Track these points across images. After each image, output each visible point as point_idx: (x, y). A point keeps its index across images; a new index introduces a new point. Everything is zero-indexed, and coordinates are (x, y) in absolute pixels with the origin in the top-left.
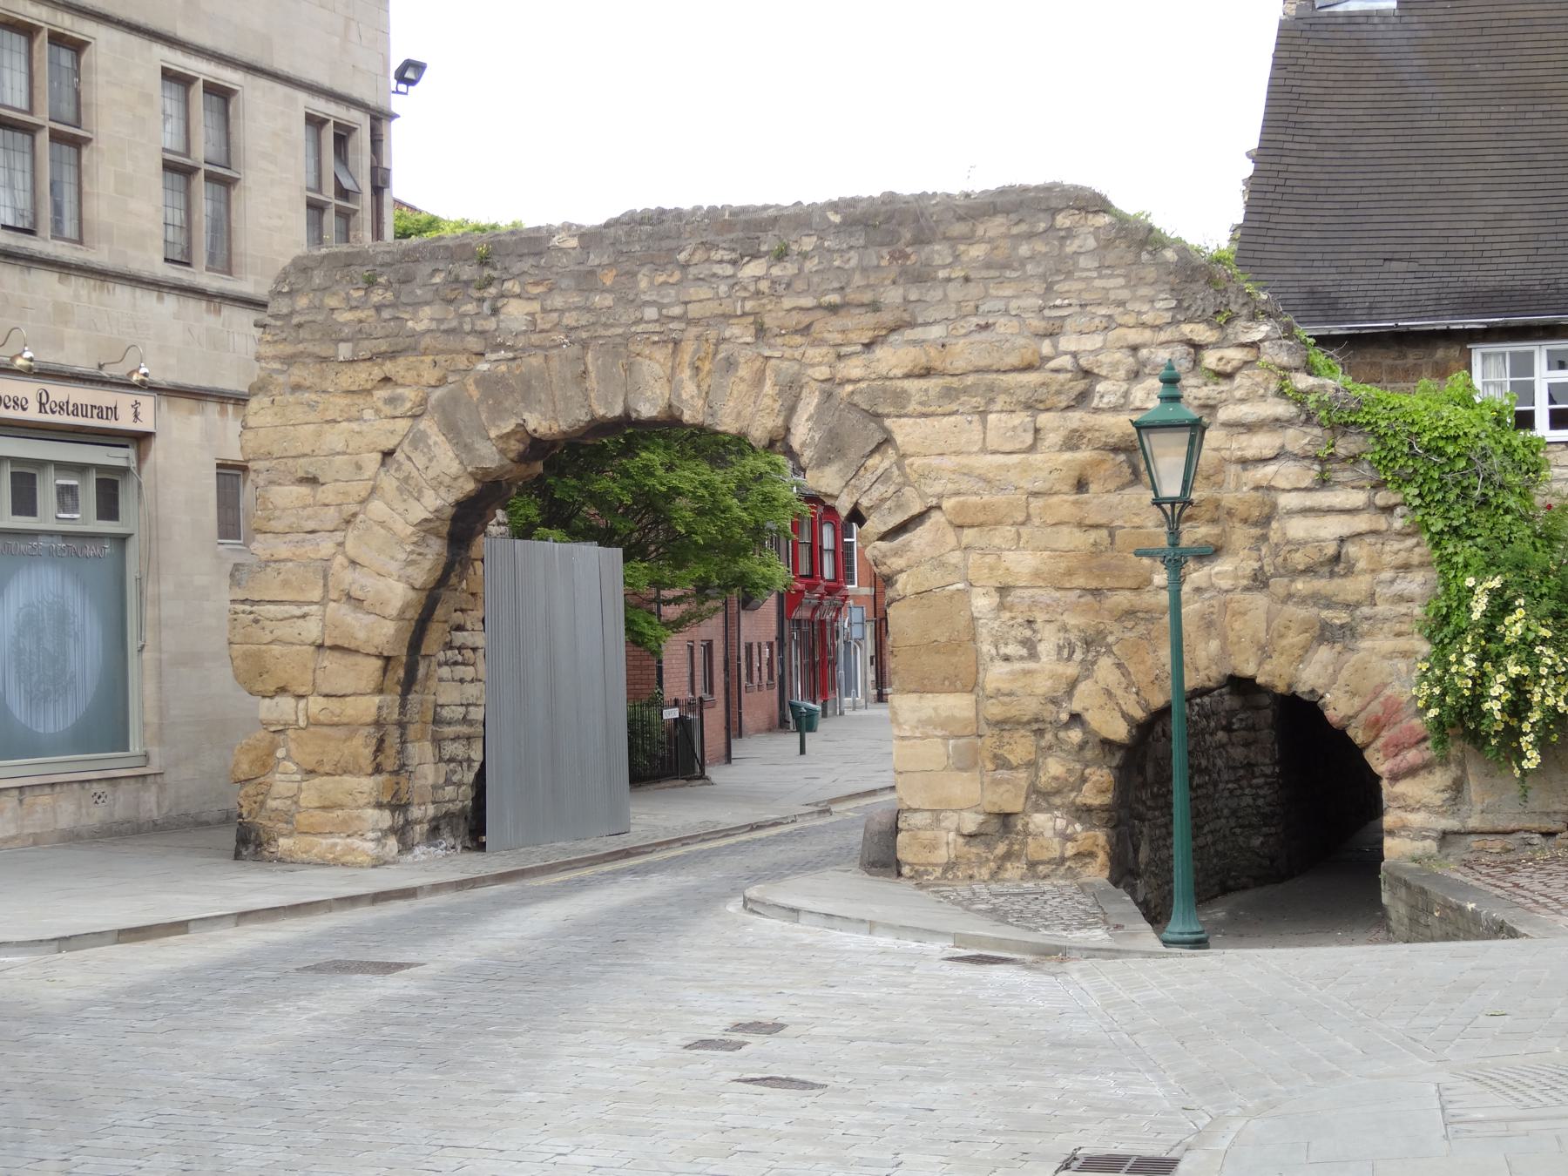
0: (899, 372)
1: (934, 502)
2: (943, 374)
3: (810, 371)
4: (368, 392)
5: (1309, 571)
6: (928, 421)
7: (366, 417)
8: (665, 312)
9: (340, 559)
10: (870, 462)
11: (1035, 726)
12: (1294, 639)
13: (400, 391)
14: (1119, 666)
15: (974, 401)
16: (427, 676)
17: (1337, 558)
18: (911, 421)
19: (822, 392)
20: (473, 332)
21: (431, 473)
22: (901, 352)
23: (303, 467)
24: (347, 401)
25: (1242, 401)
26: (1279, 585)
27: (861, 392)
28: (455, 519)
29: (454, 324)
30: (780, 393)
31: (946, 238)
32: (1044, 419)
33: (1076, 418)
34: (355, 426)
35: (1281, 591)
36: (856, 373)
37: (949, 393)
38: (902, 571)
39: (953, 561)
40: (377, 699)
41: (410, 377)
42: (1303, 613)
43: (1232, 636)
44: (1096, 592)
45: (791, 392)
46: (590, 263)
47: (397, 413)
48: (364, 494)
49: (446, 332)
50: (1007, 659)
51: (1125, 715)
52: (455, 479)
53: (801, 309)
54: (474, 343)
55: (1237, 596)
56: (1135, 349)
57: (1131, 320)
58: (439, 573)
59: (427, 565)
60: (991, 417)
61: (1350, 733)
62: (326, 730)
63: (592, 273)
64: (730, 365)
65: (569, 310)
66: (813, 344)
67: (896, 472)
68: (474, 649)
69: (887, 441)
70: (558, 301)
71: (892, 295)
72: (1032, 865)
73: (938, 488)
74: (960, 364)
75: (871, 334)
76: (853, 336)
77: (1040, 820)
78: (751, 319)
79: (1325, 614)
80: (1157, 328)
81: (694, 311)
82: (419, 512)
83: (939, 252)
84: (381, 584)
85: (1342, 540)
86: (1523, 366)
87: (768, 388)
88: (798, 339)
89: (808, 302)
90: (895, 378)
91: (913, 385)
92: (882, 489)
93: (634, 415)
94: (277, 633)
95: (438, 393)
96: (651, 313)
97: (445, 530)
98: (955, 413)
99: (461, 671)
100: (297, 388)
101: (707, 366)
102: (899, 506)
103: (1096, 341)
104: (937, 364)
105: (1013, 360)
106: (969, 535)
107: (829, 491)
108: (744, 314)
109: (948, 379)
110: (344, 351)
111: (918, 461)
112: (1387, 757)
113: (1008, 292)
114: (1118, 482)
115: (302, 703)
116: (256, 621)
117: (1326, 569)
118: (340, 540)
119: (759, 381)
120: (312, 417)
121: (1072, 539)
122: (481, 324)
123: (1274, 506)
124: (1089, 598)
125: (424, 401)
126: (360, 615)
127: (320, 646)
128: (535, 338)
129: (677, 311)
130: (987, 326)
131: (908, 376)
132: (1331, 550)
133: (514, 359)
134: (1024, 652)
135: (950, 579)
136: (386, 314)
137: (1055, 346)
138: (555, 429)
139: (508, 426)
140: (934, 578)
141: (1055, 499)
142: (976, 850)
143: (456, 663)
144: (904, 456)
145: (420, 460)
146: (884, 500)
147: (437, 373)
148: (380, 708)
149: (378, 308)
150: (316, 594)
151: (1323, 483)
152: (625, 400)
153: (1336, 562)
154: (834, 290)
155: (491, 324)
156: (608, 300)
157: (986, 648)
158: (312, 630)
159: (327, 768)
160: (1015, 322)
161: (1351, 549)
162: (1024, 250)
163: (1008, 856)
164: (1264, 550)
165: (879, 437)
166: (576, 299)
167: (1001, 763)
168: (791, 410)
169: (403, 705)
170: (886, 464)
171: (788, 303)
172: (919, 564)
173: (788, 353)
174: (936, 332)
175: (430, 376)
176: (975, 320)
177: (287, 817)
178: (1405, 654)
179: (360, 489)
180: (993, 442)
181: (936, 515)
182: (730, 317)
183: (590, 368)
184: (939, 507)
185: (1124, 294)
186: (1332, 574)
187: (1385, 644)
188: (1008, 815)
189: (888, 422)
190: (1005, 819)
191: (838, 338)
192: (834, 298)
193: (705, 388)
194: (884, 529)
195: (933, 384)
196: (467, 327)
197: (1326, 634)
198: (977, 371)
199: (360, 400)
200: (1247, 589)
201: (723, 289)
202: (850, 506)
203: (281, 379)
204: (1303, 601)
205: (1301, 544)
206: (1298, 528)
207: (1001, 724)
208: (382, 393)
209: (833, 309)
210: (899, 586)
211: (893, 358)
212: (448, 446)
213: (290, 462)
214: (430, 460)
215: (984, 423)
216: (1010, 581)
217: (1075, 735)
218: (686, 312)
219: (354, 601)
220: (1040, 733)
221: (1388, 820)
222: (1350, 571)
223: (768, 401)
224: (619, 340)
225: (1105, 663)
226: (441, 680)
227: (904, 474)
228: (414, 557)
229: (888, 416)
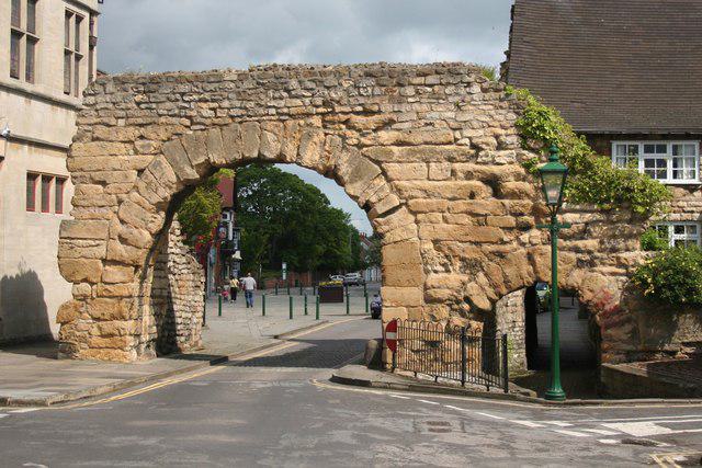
0: (389, 143)
1: (404, 201)
11: (448, 302)
14: (486, 275)
20: (186, 117)
23: (98, 176)
24: (122, 145)
29: (177, 111)
31: (410, 84)
32: (457, 166)
33: (471, 166)
34: (126, 158)
36: (369, 142)
37: (414, 153)
41: (153, 136)
42: (573, 256)
44: (477, 243)
50: (436, 272)
54: (188, 122)
55: (543, 247)
57: (496, 124)
60: (433, 165)
62: (108, 300)
69: (384, 173)
70: (226, 104)
71: (387, 107)
74: (419, 139)
79: (580, 255)
81: (293, 111)
82: (156, 199)
83: (410, 91)
84: (135, 231)
85: (587, 224)
89: (347, 109)
94: (83, 253)
96: (273, 111)
100: (98, 139)
103: (481, 132)
105: (442, 139)
106: (420, 216)
110: (121, 122)
115: (94, 287)
116: (72, 248)
120: (105, 152)
121: (467, 220)
122: (189, 113)
124: (474, 246)
127: (105, 261)
128: (216, 121)
129: (286, 110)
130: (431, 124)
136: (143, 106)
137: (461, 134)
139: (202, 159)
141: (459, 201)
142: (415, 357)
149: (138, 104)
150: (105, 235)
154: (360, 105)
155: (194, 113)
158: (101, 251)
159: (106, 317)
162: (448, 90)
163: (436, 360)
166: (238, 104)
169: (141, 288)
174: (406, 126)
177: (83, 339)
184: (406, 204)
185: (493, 112)
186: (582, 238)
190: (433, 344)
192: (360, 109)
197: (580, 264)
198: (426, 143)
201: (307, 101)
203: (89, 134)
205: (567, 225)
206: (569, 217)
208: (139, 143)
211: (385, 136)
213: (93, 174)
215: (428, 167)
216: (438, 237)
217: (466, 306)
219: (123, 240)
220: (450, 305)
225: (481, 274)
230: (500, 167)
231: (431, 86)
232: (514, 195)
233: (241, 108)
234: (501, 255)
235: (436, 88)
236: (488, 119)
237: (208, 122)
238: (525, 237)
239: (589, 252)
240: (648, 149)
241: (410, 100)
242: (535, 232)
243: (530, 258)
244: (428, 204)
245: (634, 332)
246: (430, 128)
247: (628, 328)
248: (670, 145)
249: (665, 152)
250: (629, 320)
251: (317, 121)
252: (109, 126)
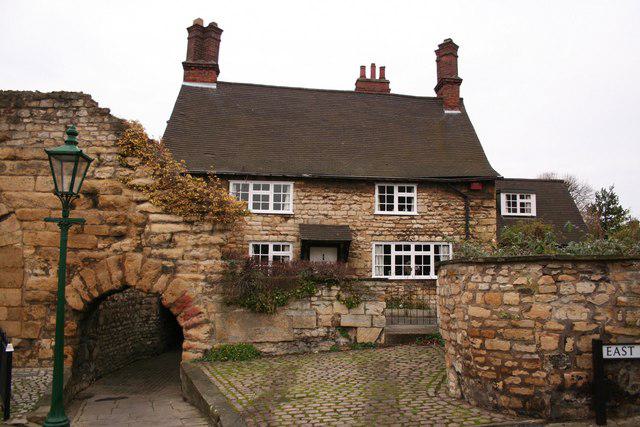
1: (12, 210)
2: (20, 159)
5: (159, 246)
12: (153, 272)
15: (33, 170)
17: (170, 241)
25: (138, 177)
26: (148, 250)
31: (28, 107)
35: (148, 253)
37: (23, 167)
43: (127, 270)
50: (36, 275)
51: (83, 300)
56: (98, 155)
57: (98, 143)
61: (171, 310)
72: (40, 360)
77: (44, 342)
79: (164, 262)
80: (107, 147)
83: (25, 113)
85: (172, 234)
86: (246, 188)
91: (8, 163)
104: (19, 156)
111: (8, 193)
112: (185, 320)
113: (51, 129)
114: (88, 206)
117: (166, 245)
123: (148, 219)
130: (41, 142)
131: (5, 159)
132: (168, 237)
134: (44, 273)
140: (10, 241)
151: (166, 212)
153: (171, 242)
157: (28, 270)
160: (52, 141)
161: (176, 237)
162: (59, 114)
164: (142, 236)
167: (30, 317)
178: (195, 280)
180: (39, 188)
181: (13, 216)
185: (96, 133)
186: (168, 247)
187: (187, 276)
188: (32, 340)
190: (31, 340)
195: (16, 163)
197: (165, 270)
198: (35, 159)
200: (134, 251)
204: (156, 257)
206: (156, 228)
207: (33, 301)
216: (40, 244)
221: (185, 344)
222: (175, 246)
230: (101, 182)
231: (45, 109)
232: (110, 207)
234: (95, 260)
235: (50, 111)
236: (92, 139)
238: (116, 245)
239: (173, 260)
240: (256, 188)
241: (25, 120)
242: (127, 241)
243: (121, 265)
244: (32, 213)
245: (212, 332)
246: (38, 145)
247: (206, 328)
248: (272, 185)
249: (268, 189)
250: (207, 322)
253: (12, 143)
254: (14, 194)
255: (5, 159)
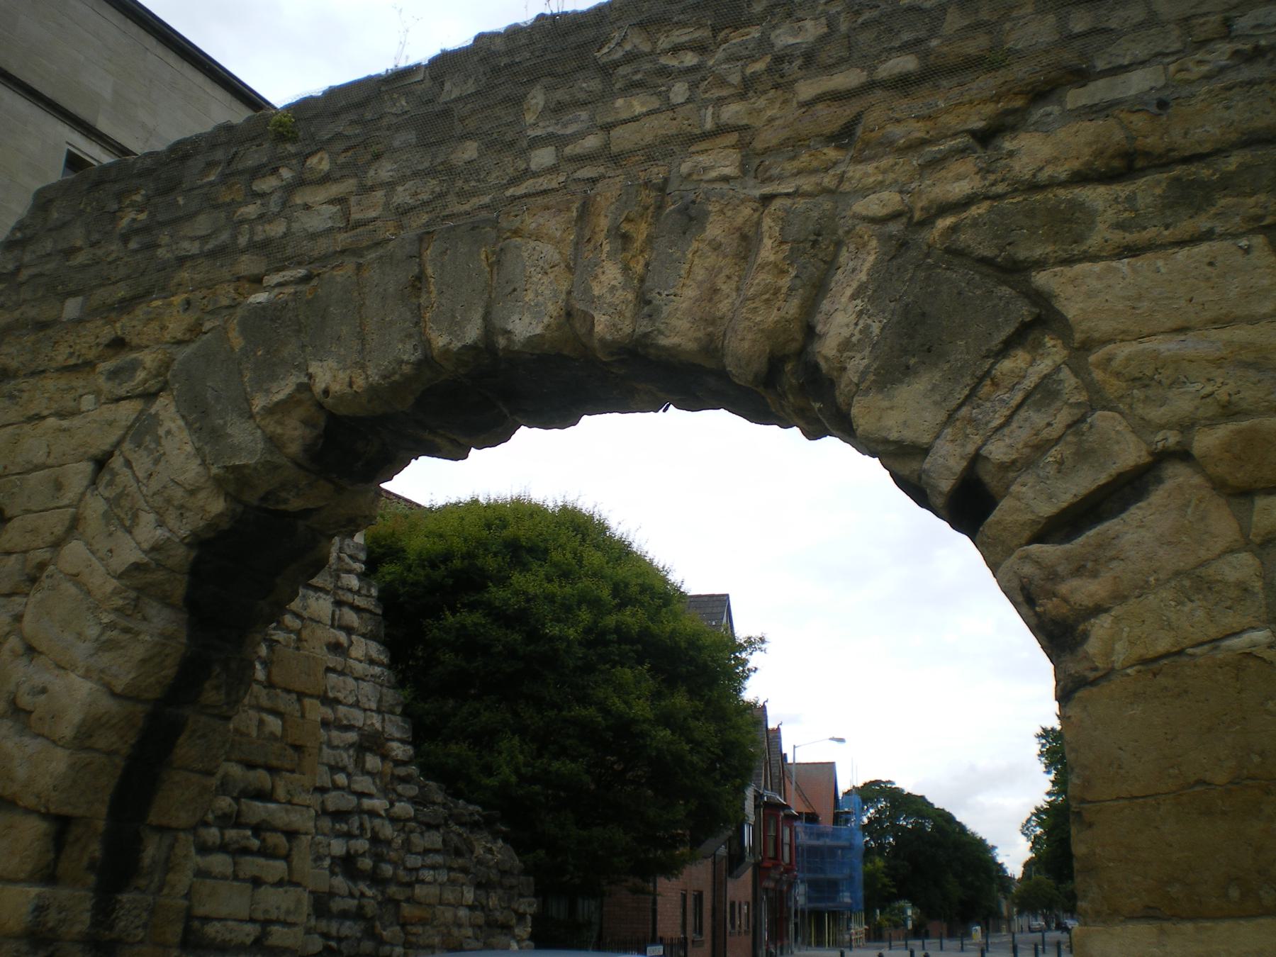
0: (1062, 172)
1: (1172, 439)
2: (1162, 161)
3: (860, 207)
4: (89, 365)
6: (1140, 262)
7: (84, 407)
8: (568, 150)
9: (13, 642)
10: (1006, 365)
13: (134, 355)
16: (168, 865)
18: (1098, 267)
19: (885, 239)
21: (154, 485)
22: (1062, 134)
27: (975, 223)
28: (196, 572)
29: (224, 236)
30: (791, 258)
36: (960, 189)
37: (1190, 196)
38: (1098, 610)
39: (1232, 576)
40: (34, 891)
45: (817, 252)
46: (444, 98)
47: (122, 391)
48: (59, 530)
49: (212, 254)
52: (192, 493)
53: (836, 97)
58: (170, 671)
59: (139, 652)
63: (446, 113)
64: (691, 218)
65: (403, 179)
66: (857, 160)
67: (1069, 380)
68: (292, 834)
69: (1043, 319)
70: (385, 171)
73: (1182, 404)
75: (989, 109)
76: (951, 121)
78: (733, 138)
81: (624, 138)
82: (129, 552)
87: (767, 252)
88: (831, 153)
90: (1052, 183)
91: (1095, 196)
92: (1039, 419)
93: (502, 342)
95: (188, 350)
96: (543, 157)
97: (179, 590)
98: (1208, 236)
99: (252, 865)
101: (641, 231)
102: (1084, 455)
104: (1152, 142)
107: (909, 435)
108: (721, 130)
109: (1178, 171)
110: (72, 308)
111: (1124, 351)
118: (19, 609)
119: (747, 241)
125: (166, 365)
126: (27, 740)
129: (592, 142)
131: (1081, 178)
133: (307, 279)
135: (1231, 620)
138: (360, 382)
139: (284, 389)
140: (1194, 620)
143: (246, 851)
144: (1087, 346)
145: (142, 463)
146: (1041, 447)
147: (189, 318)
148: (40, 909)
152: (487, 317)
154: (904, 48)
155: (276, 229)
156: (470, 150)
165: (1025, 311)
168: (819, 289)
169: (104, 910)
170: (1044, 366)
171: (806, 90)
172: (1143, 589)
173: (807, 184)
174: (1138, 82)
175: (176, 325)
176: (1226, 48)
179: (55, 522)
181: (1178, 476)
182: (692, 139)
183: (429, 271)
184: (1183, 455)
189: (1041, 279)
191: (918, 130)
193: (639, 268)
194: (1047, 509)
196: (243, 241)
199: (79, 382)
201: (679, 91)
202: (958, 465)
209: (903, 84)
210: (1092, 647)
212: (185, 435)
214: (157, 462)
218: (607, 145)
223: (764, 278)
224: (484, 214)
226: (202, 874)
227: (1090, 386)
228: (109, 634)
229: (1041, 264)
233: (431, 172)
237: (323, 246)
251: (721, 161)
252: (42, 326)
253: (1097, 91)
254: (1167, 346)
255: (1081, 178)
